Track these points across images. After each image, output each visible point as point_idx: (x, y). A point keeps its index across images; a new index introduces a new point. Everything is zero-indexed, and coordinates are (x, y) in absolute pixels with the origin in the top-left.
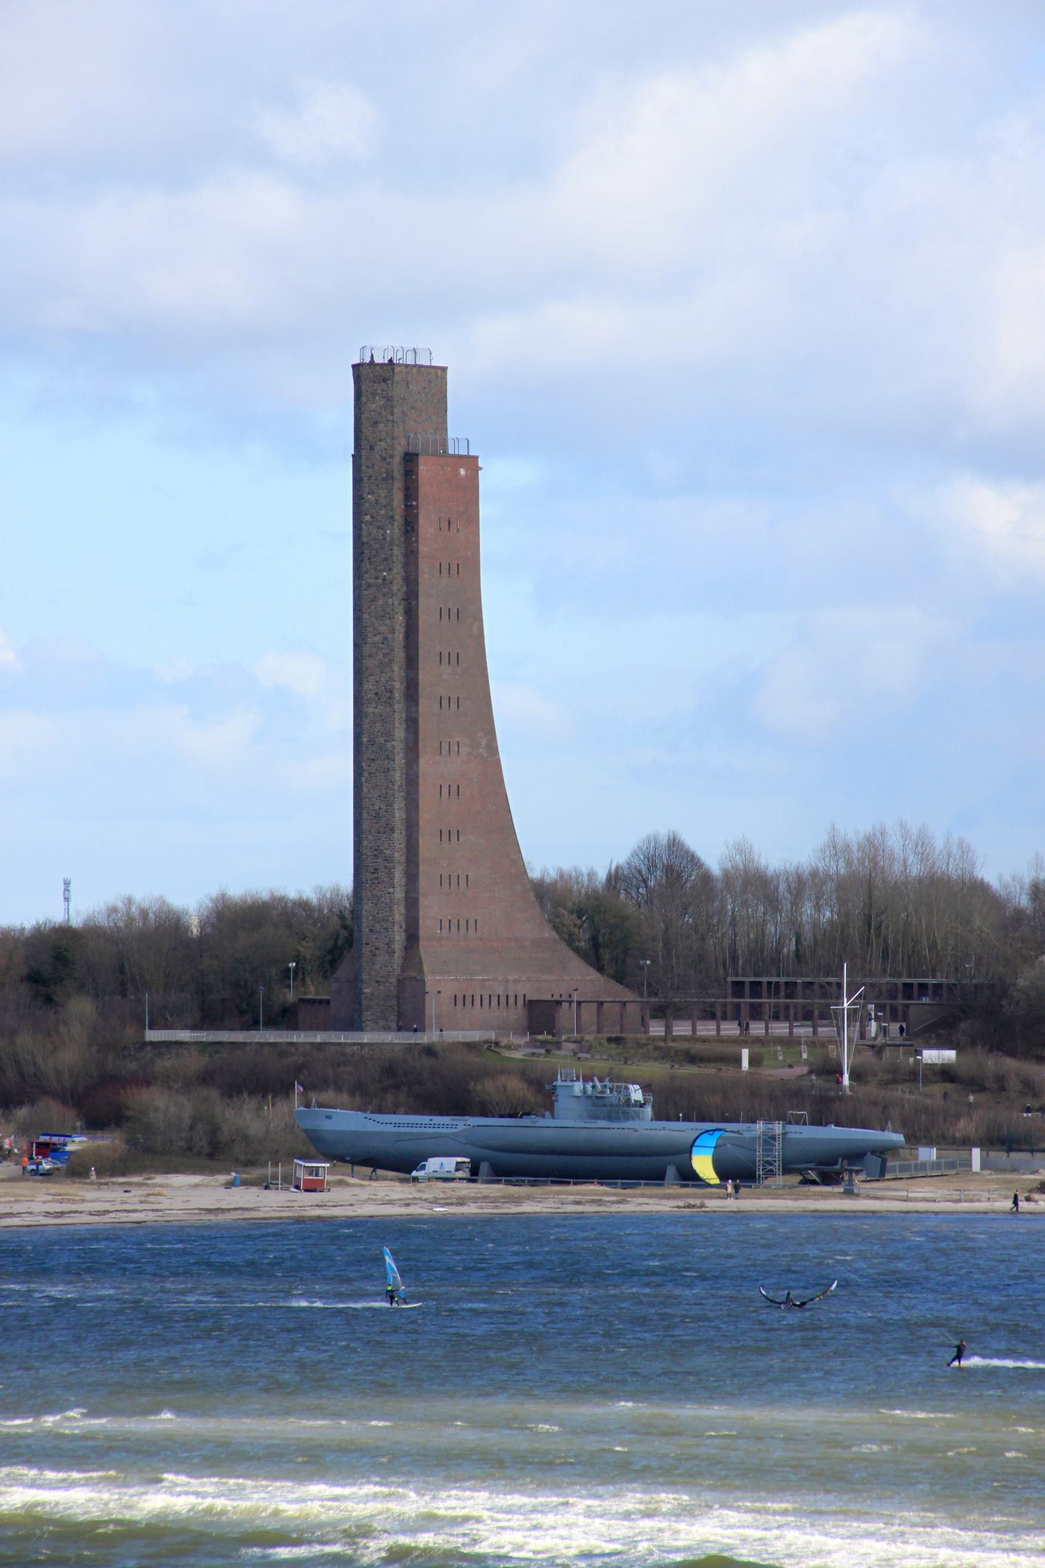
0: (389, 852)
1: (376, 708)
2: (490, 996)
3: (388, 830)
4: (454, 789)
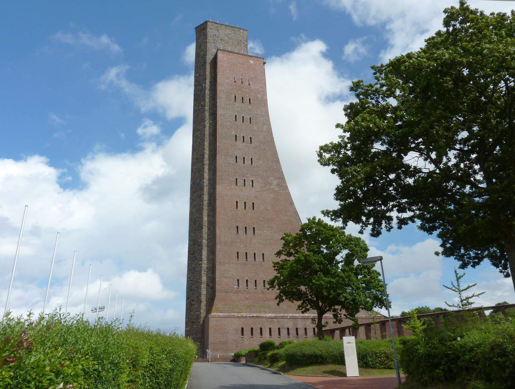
0: (200, 240)
1: (196, 166)
2: (279, 329)
4: (249, 205)
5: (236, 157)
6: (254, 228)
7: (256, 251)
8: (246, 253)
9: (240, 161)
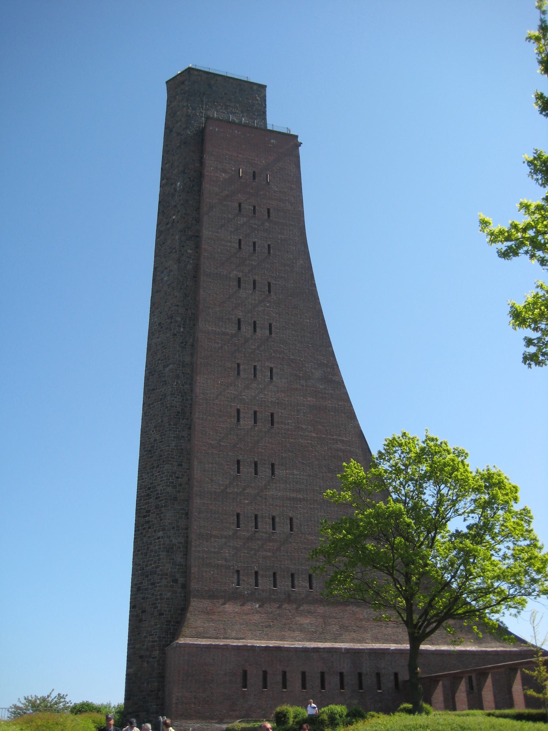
1: (158, 338)
2: (322, 674)
6: (273, 465)
8: (256, 517)
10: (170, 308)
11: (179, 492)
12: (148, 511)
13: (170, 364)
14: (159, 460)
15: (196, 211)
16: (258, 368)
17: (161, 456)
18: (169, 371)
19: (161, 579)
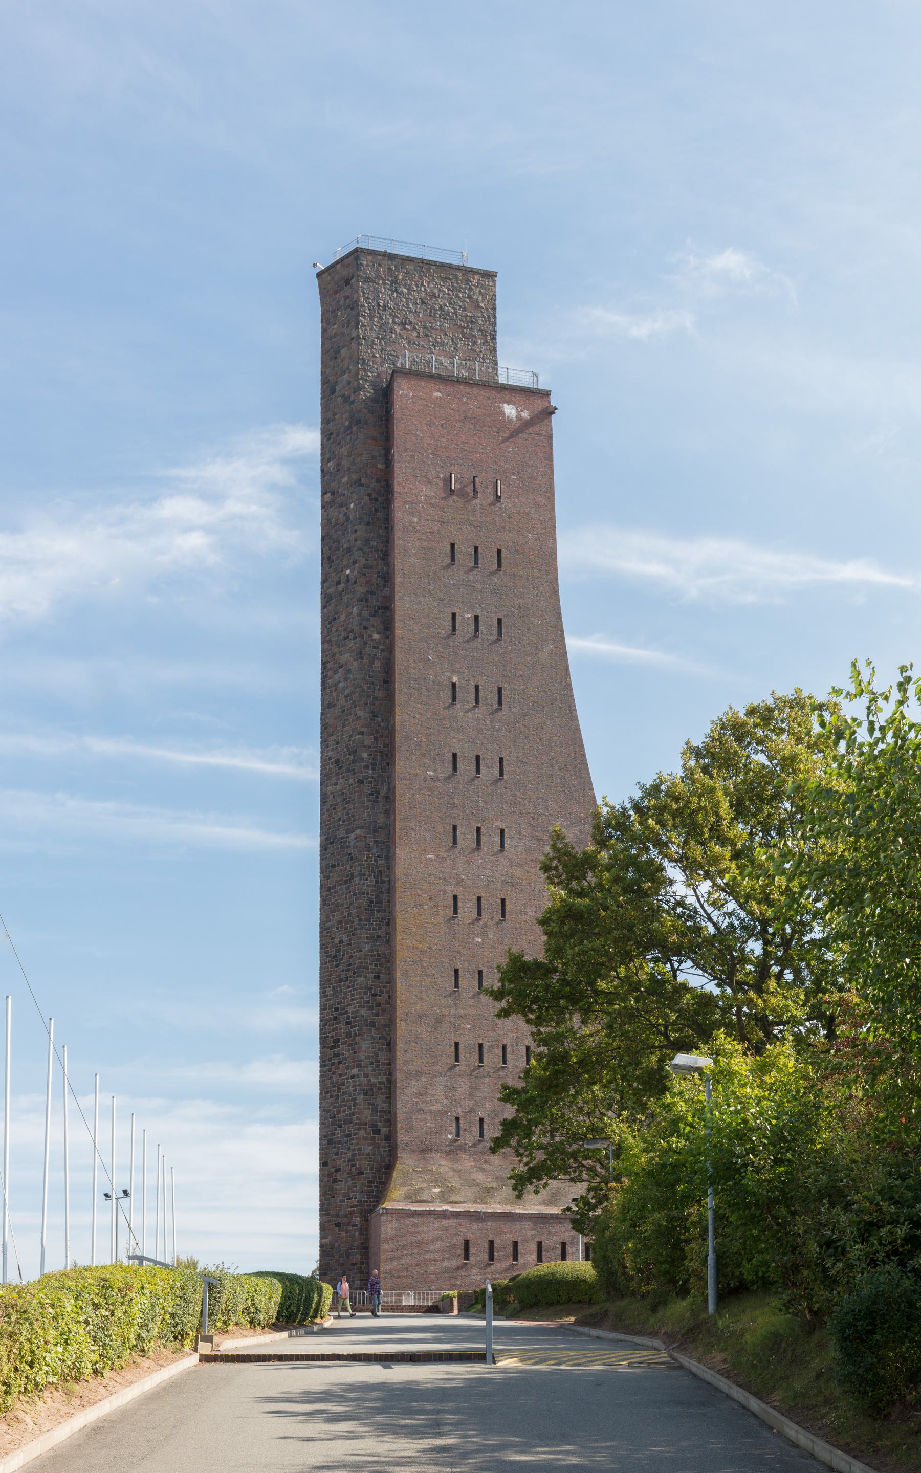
1: (336, 784)
3: (351, 973)
4: (491, 905)
5: (455, 755)
7: (507, 1041)
9: (466, 767)
10: (351, 736)
11: (377, 1015)
12: (338, 1041)
13: (356, 828)
14: (348, 970)
15: (383, 559)
16: (482, 829)
17: (350, 965)
18: (356, 838)
19: (359, 1129)
